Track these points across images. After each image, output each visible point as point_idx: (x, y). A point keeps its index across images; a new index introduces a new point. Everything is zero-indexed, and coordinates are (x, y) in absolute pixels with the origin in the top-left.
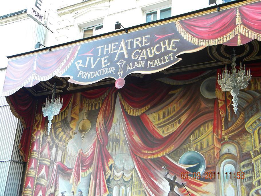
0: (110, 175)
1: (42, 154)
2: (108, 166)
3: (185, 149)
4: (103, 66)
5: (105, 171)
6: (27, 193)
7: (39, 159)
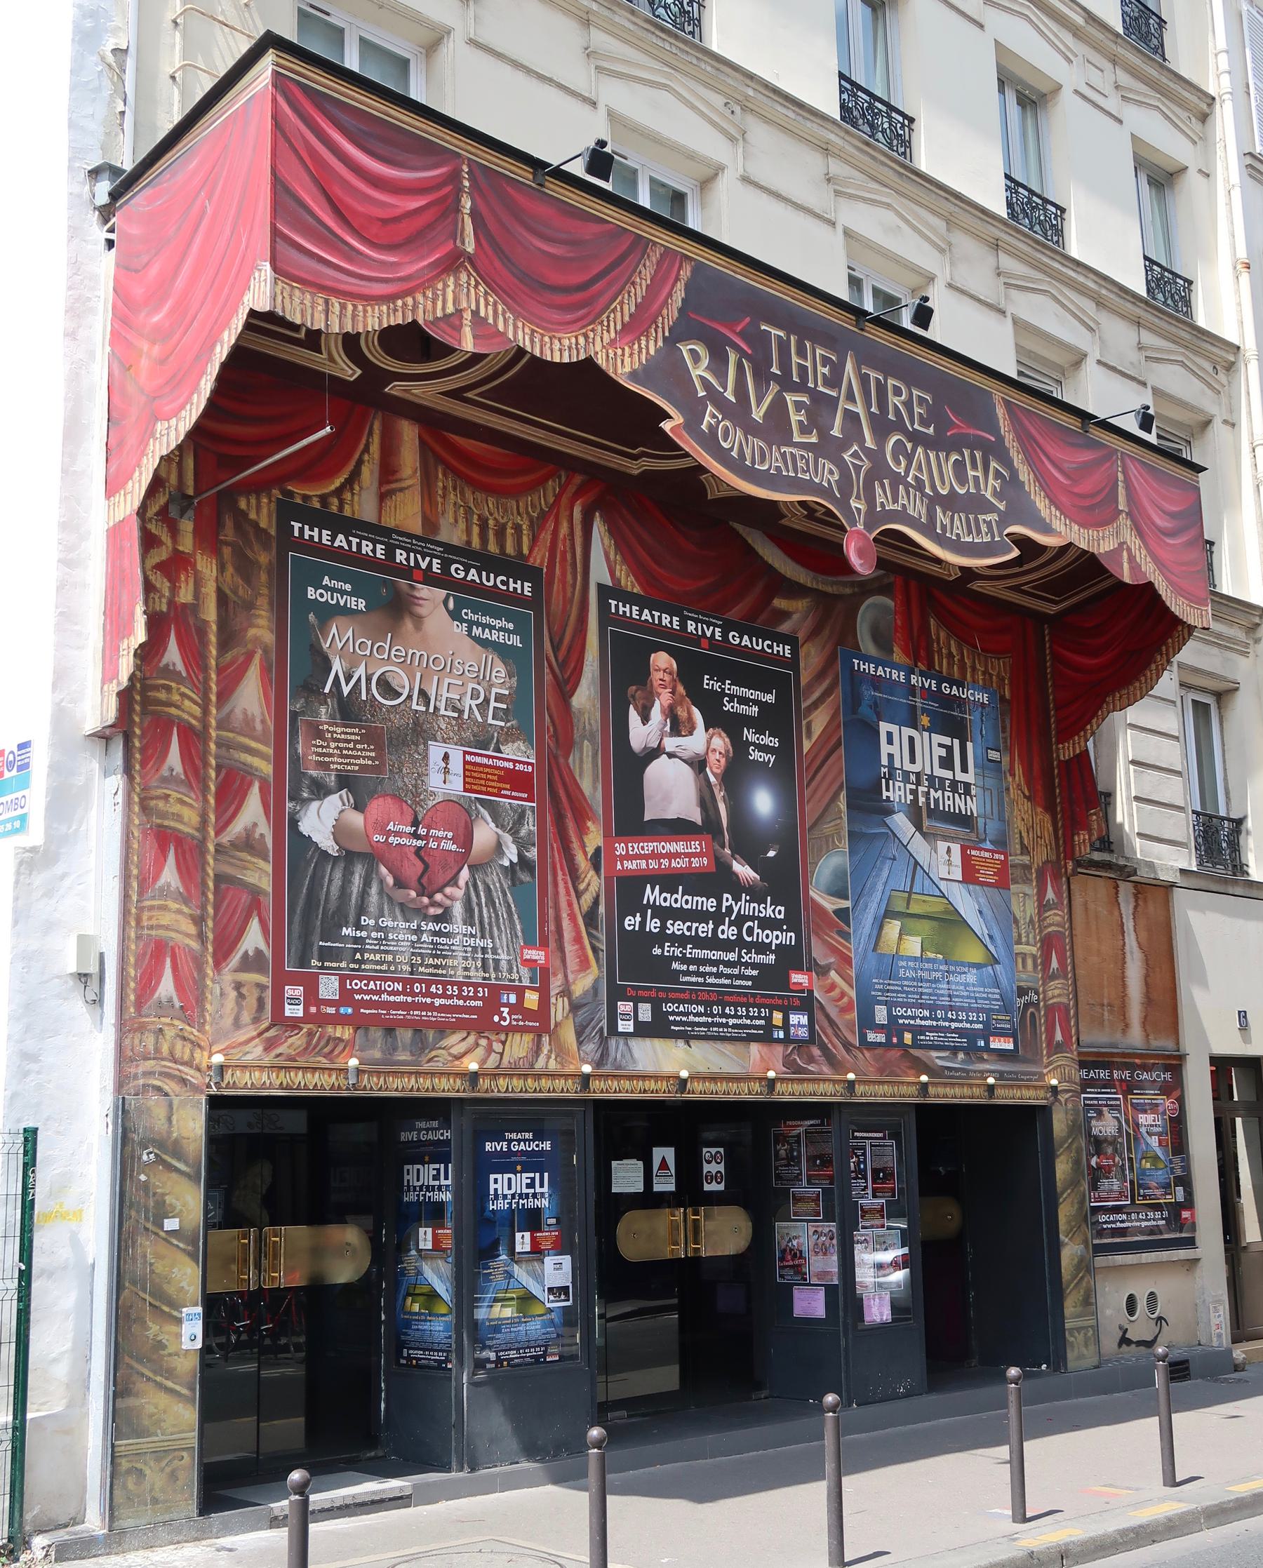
0: (598, 896)
1: (232, 711)
2: (585, 853)
3: (827, 837)
4: (797, 438)
6: (167, 928)
7: (213, 734)
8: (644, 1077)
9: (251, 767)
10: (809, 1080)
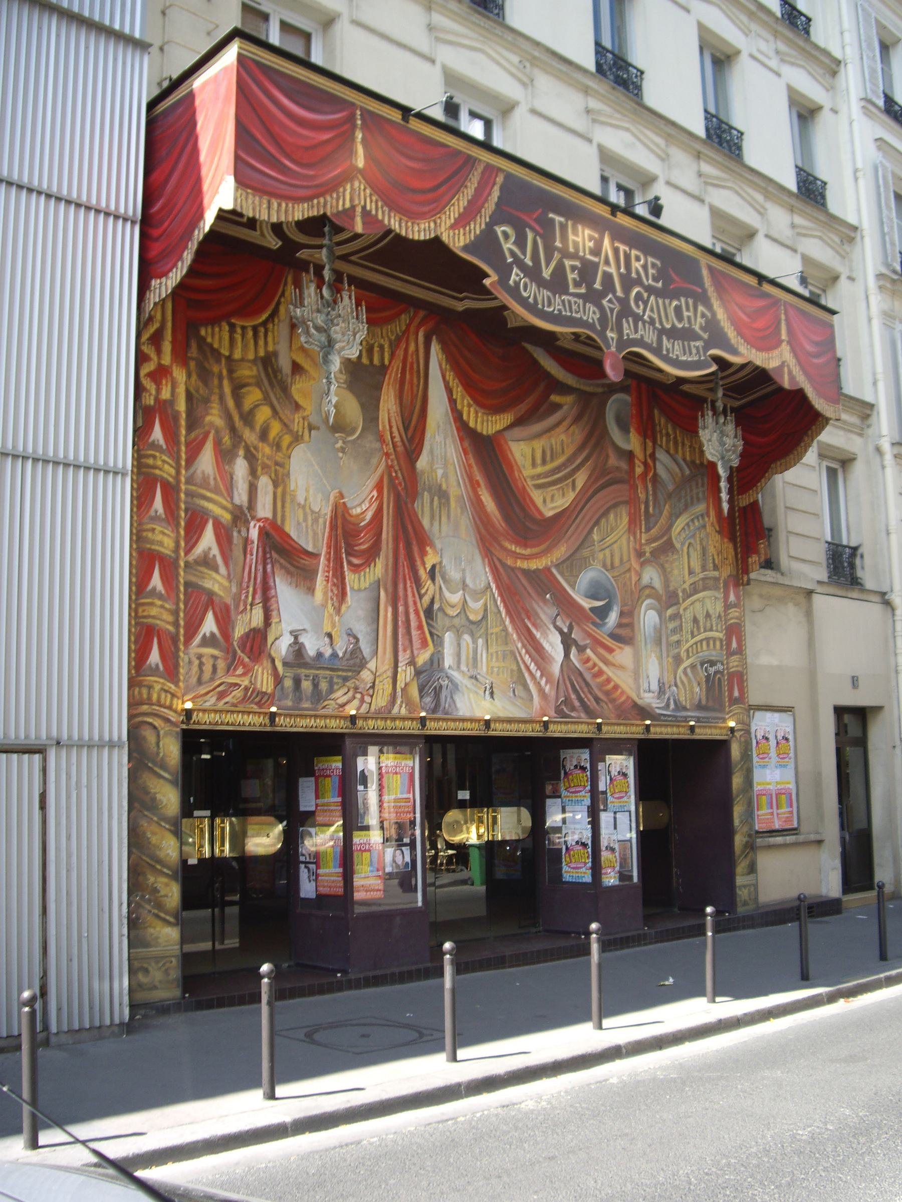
3: (585, 558)
4: (572, 290)
5: (418, 583)
6: (154, 617)
7: (183, 487)
8: (463, 720)
9: (207, 509)
10: (572, 722)
